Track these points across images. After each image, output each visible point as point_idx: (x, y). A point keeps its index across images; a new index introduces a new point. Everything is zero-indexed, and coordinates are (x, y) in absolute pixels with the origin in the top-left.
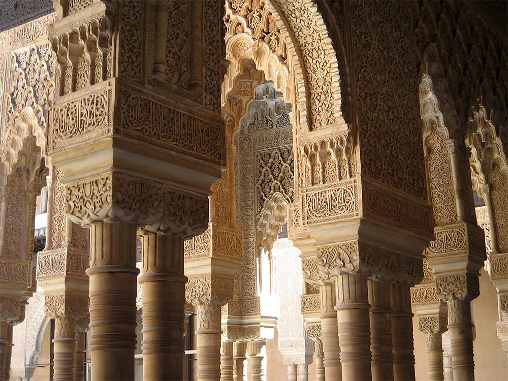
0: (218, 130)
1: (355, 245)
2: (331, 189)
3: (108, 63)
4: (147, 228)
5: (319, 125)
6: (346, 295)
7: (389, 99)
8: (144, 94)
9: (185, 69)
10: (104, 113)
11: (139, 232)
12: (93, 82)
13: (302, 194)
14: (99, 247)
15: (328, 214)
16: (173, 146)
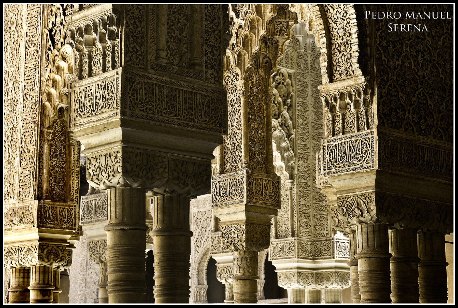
0: (219, 101)
1: (372, 195)
2: (350, 140)
3: (116, 54)
4: (155, 190)
5: (339, 76)
6: (365, 244)
7: (418, 43)
8: (147, 78)
9: (186, 50)
10: (113, 98)
11: (149, 194)
12: (104, 70)
13: (324, 144)
14: (113, 209)
15: (346, 165)
16: (176, 120)
